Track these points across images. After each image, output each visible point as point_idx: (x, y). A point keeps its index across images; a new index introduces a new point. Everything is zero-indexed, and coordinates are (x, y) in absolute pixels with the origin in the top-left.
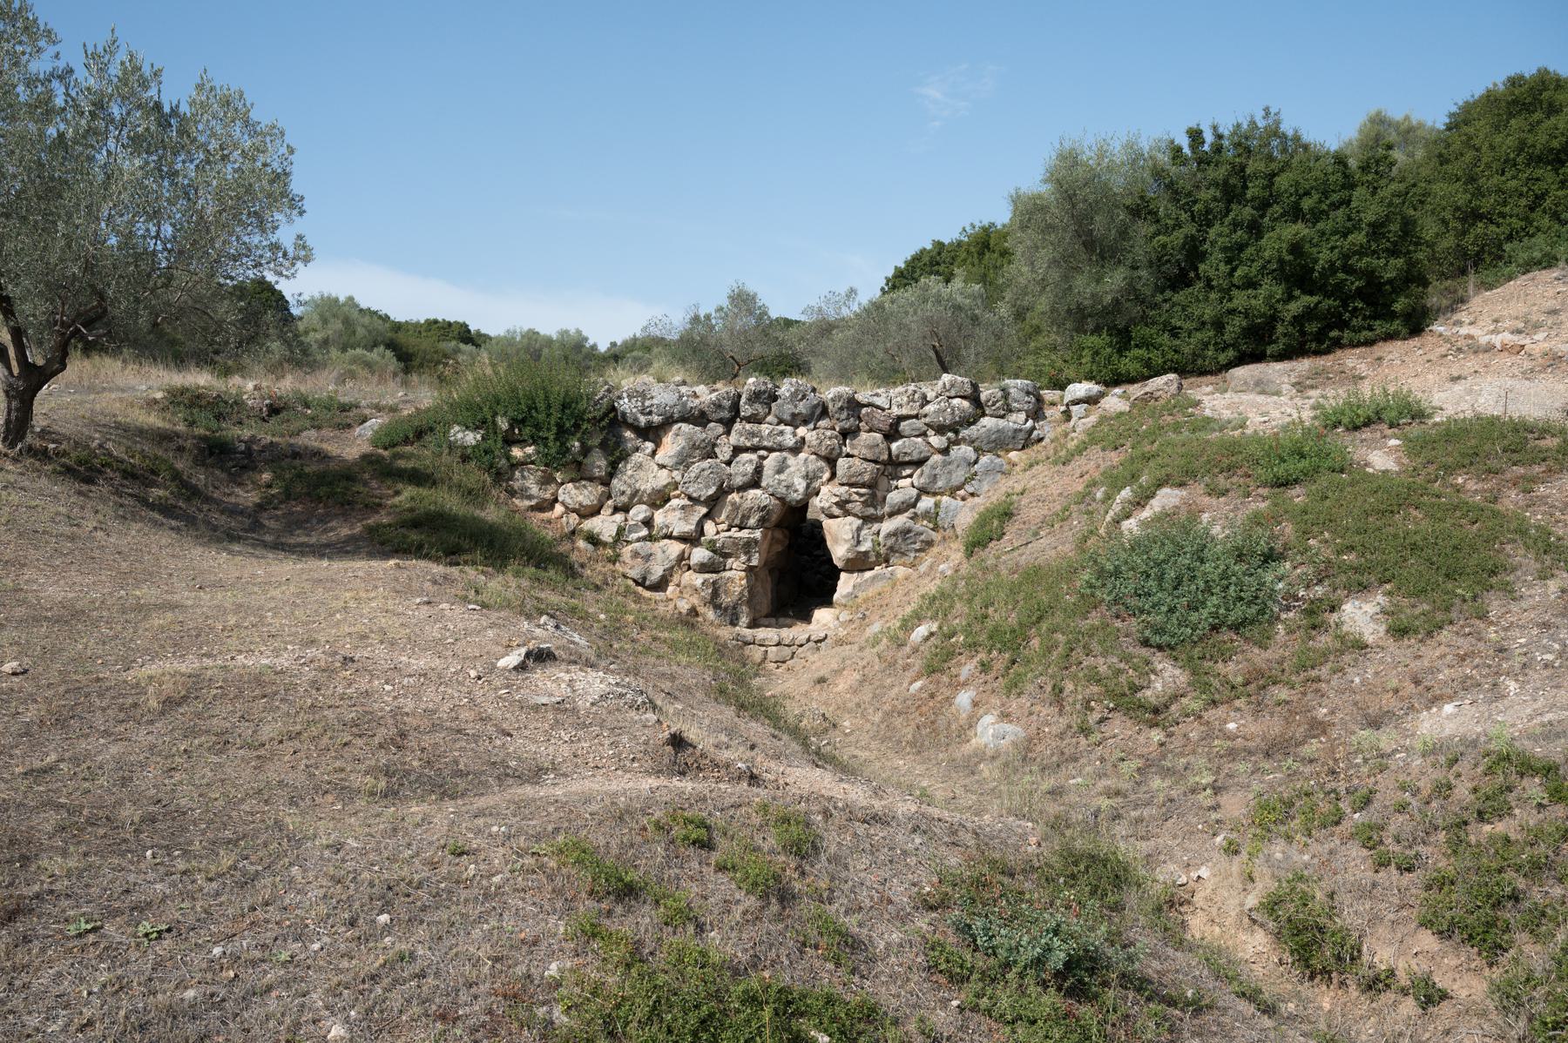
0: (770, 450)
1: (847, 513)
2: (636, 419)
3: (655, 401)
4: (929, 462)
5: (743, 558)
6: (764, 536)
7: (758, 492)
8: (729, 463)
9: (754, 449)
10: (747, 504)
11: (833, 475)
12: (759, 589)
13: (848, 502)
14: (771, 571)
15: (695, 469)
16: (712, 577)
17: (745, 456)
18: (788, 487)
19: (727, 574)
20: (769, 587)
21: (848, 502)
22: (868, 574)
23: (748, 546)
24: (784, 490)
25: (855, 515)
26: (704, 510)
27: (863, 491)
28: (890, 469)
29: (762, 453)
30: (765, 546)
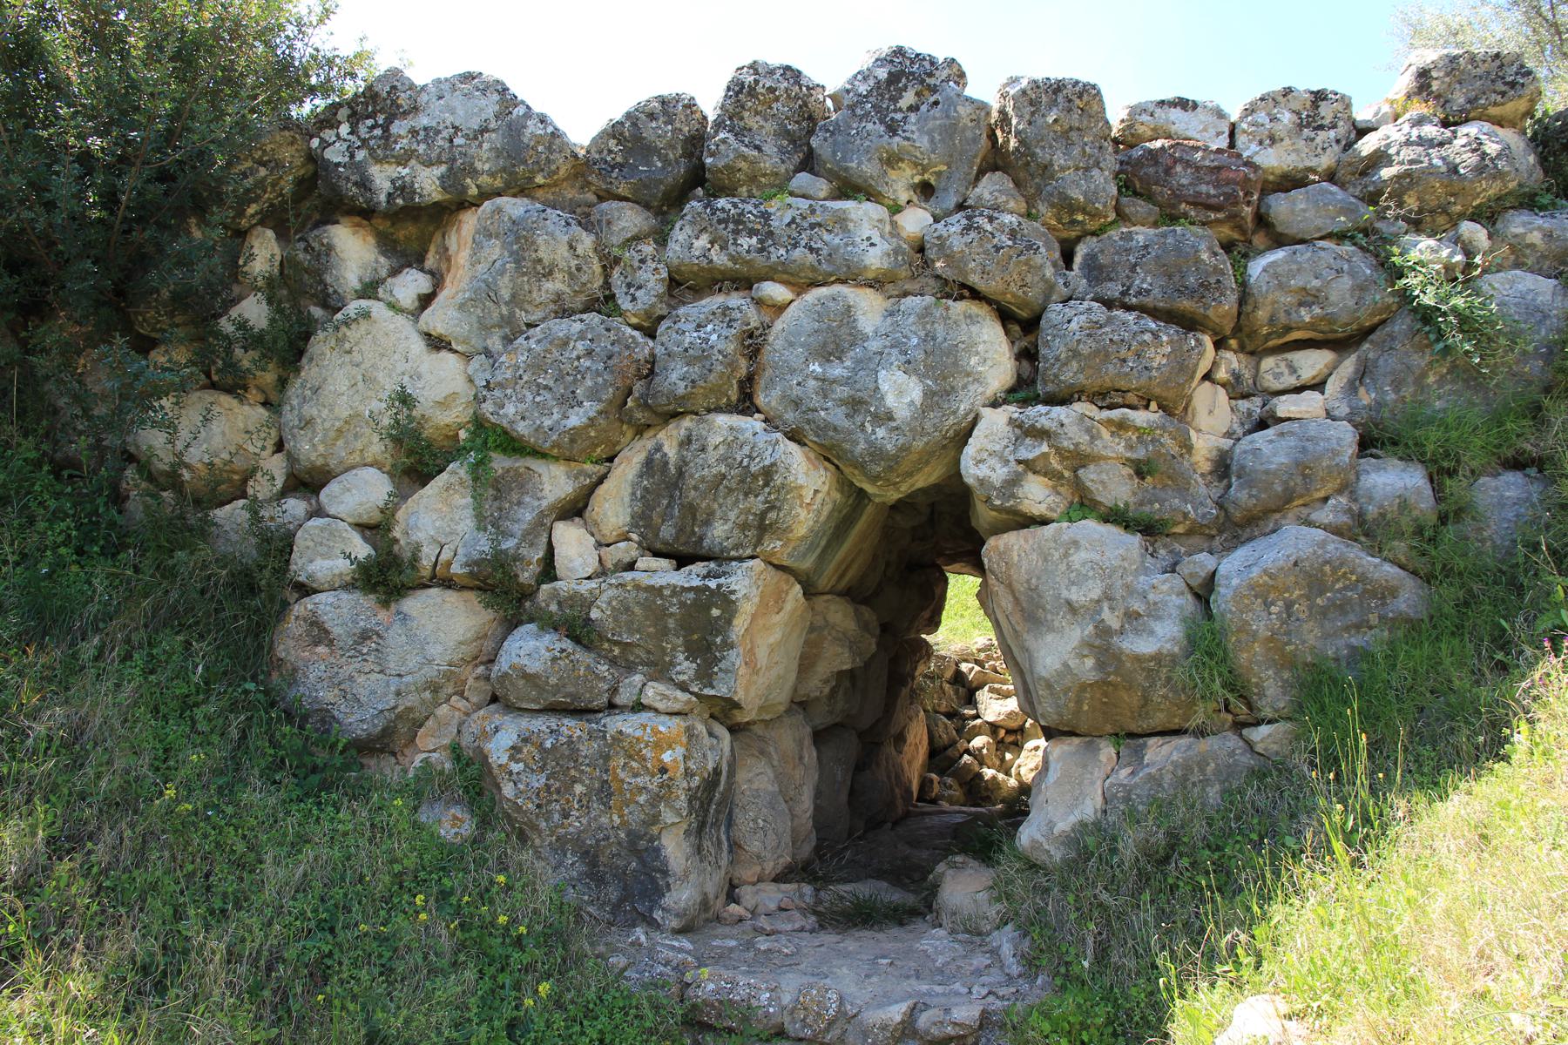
0: (802, 282)
1: (1084, 504)
2: (365, 184)
3: (423, 121)
5: (686, 668)
7: (752, 425)
9: (744, 282)
10: (709, 465)
15: (532, 343)
19: (626, 724)
22: (1159, 753)
25: (1114, 516)
26: (556, 482)
29: (774, 291)
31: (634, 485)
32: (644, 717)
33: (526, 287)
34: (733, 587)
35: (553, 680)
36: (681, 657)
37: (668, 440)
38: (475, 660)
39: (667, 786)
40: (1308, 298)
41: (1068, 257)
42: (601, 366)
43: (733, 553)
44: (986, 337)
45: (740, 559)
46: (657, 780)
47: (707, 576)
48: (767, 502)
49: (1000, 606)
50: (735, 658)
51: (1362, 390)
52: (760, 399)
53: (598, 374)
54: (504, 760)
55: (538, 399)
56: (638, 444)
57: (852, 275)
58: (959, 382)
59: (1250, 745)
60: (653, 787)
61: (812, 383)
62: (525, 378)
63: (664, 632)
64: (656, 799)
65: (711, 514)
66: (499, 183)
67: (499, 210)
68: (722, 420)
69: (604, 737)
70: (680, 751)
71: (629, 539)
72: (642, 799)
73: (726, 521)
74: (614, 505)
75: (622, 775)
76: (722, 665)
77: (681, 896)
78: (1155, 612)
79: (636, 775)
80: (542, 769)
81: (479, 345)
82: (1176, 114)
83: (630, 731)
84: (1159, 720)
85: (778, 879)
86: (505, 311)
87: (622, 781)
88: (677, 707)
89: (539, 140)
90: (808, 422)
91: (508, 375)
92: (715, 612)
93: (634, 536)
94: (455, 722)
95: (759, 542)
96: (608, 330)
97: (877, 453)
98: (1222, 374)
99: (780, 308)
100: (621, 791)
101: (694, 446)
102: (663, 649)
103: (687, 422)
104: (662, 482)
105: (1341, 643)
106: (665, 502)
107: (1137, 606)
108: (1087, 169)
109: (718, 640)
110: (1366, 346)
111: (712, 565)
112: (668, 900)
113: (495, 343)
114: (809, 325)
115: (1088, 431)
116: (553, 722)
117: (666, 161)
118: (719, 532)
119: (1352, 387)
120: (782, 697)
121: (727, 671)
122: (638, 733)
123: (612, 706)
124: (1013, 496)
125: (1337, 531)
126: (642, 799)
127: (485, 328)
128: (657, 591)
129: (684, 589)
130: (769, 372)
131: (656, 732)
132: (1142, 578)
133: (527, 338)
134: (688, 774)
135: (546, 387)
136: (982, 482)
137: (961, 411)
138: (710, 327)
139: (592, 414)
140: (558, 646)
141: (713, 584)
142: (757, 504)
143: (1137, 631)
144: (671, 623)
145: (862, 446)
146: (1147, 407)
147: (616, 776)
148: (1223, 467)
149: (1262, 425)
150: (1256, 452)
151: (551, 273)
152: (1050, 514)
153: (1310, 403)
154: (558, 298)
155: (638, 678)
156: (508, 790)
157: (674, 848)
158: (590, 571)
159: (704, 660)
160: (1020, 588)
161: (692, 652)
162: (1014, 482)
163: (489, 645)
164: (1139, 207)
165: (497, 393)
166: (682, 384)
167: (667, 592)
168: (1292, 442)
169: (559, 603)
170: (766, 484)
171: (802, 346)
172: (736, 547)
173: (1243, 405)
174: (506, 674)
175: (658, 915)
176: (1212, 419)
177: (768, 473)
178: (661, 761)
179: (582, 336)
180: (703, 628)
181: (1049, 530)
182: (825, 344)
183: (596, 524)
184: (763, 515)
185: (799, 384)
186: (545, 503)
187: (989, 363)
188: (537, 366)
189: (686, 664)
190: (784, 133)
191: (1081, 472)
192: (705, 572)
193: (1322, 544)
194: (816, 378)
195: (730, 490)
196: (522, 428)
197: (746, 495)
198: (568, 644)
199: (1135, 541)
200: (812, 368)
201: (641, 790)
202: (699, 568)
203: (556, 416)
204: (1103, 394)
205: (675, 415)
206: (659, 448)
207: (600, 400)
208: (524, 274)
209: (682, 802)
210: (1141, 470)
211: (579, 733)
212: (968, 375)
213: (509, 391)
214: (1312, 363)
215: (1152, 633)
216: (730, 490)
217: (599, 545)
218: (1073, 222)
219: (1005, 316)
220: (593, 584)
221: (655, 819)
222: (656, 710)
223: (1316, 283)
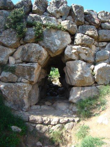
1: (79, 58)
5: (27, 77)
6: (38, 68)
11: (73, 40)
14: (39, 87)
18: (51, 43)
20: (38, 92)
26: (10, 51)
27: (87, 48)
37: (26, 46)
40: (105, 36)
41: (78, 28)
47: (31, 65)
49: (68, 70)
50: (34, 75)
54: (3, 89)
56: (21, 46)
59: (97, 88)
60: (23, 92)
66: (2, 8)
67: (3, 12)
68: (34, 44)
72: (22, 94)
73: (34, 57)
74: (18, 54)
76: (32, 76)
77: (27, 107)
82: (91, 12)
85: (36, 105)
89: (9, 3)
92: (32, 70)
95: (38, 60)
97: (54, 50)
98: (95, 44)
103: (29, 44)
104: (25, 52)
107: (86, 71)
108: (81, 17)
112: (25, 107)
116: (9, 84)
117: (27, 8)
118: (33, 59)
120: (36, 82)
123: (17, 82)
128: (24, 66)
134: (28, 91)
136: (67, 54)
141: (32, 66)
142: (38, 55)
144: (26, 71)
148: (95, 55)
150: (99, 54)
155: (20, 78)
156: (3, 93)
157: (26, 100)
158: (14, 63)
160: (71, 68)
161: (28, 75)
162: (72, 55)
164: (87, 23)
175: (23, 109)
177: (40, 51)
180: (30, 72)
181: (75, 61)
184: (39, 57)
190: (43, 7)
191: (80, 54)
195: (35, 53)
196: (5, 43)
202: (29, 64)
204: (83, 45)
205: (27, 43)
209: (27, 95)
214: (105, 44)
216: (35, 53)
217: (15, 60)
218: (79, 23)
219: (70, 34)
223: (106, 34)
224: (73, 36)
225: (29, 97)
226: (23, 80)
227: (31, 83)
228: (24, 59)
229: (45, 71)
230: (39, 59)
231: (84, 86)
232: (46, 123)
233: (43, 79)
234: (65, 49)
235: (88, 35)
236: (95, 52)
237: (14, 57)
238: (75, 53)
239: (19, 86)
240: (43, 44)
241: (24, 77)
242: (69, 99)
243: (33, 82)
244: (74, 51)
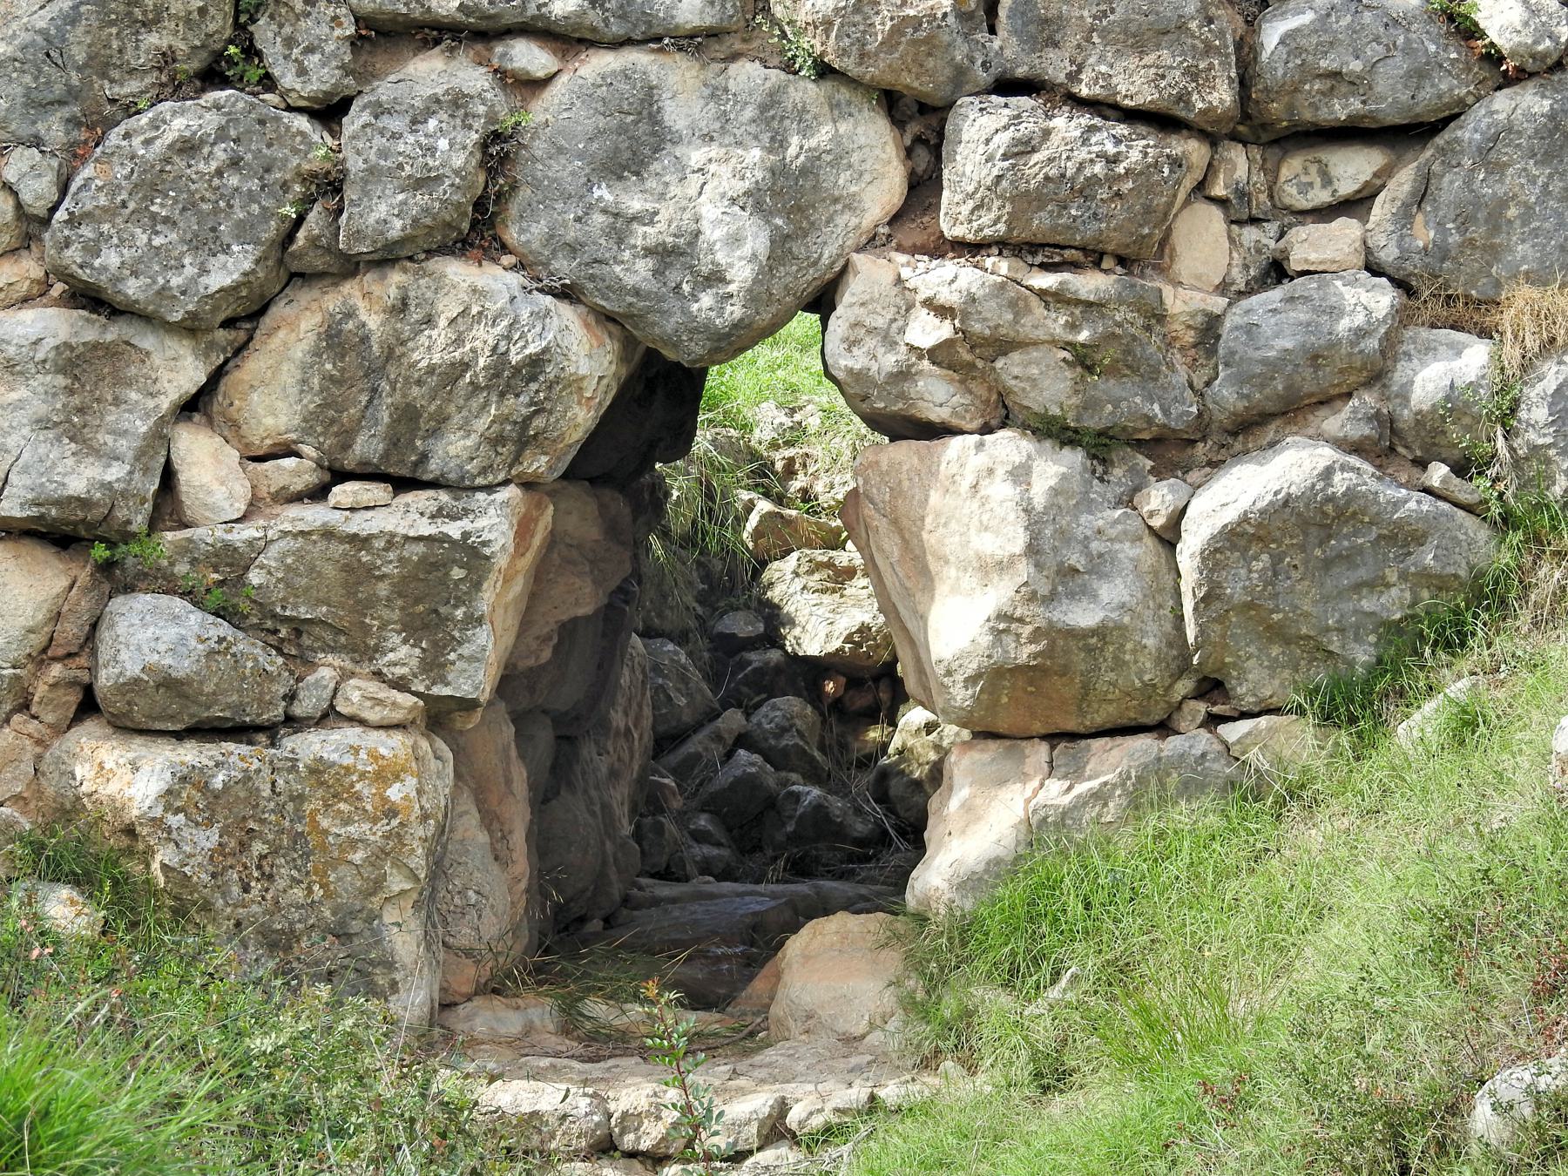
0: (569, 40)
1: (1002, 413)
4: (1468, 132)
5: (401, 655)
6: (523, 530)
8: (329, 112)
11: (923, 188)
12: (471, 829)
13: (1003, 346)
16: (227, 761)
17: (428, 73)
18: (664, 255)
19: (310, 745)
20: (518, 816)
21: (1003, 346)
22: (1111, 762)
23: (433, 588)
24: (640, 272)
26: (182, 371)
27: (1090, 284)
28: (1239, 164)
29: (529, 56)
30: (518, 586)
31: (305, 368)
32: (351, 734)
33: (115, 44)
34: (486, 536)
35: (209, 688)
36: (396, 639)
37: (365, 304)
38: (42, 657)
39: (397, 836)
42: (254, 184)
43: (480, 481)
44: (862, 140)
45: (489, 489)
46: (382, 827)
48: (532, 403)
51: (1420, 218)
52: (512, 234)
53: (251, 197)
54: (158, 812)
55: (157, 241)
56: (305, 295)
57: (656, 37)
58: (820, 215)
61: (598, 219)
62: (132, 205)
63: (370, 603)
64: (380, 855)
65: (442, 420)
69: (293, 769)
70: (411, 782)
71: (298, 455)
72: (358, 857)
75: (325, 823)
76: (466, 650)
78: (1100, 566)
79: (347, 822)
80: (210, 822)
81: (25, 131)
83: (334, 757)
84: (1101, 715)
86: (75, 78)
87: (326, 832)
88: (398, 716)
90: (592, 278)
91: (103, 201)
92: (457, 573)
93: (307, 449)
94: (28, 757)
95: (517, 460)
96: (262, 122)
99: (534, 85)
100: (324, 847)
101: (416, 315)
102: (366, 630)
105: (1348, 606)
106: (364, 398)
107: (1075, 559)
109: (459, 613)
110: (1428, 153)
111: (444, 497)
113: (54, 129)
114: (586, 120)
115: (1013, 304)
119: (1405, 217)
121: (472, 659)
122: (348, 760)
123: (293, 723)
124: (902, 396)
125: (1356, 448)
126: (358, 857)
127: (38, 105)
129: (407, 538)
130: (525, 193)
131: (375, 756)
132: (1084, 518)
133: (127, 136)
134: (425, 817)
135: (166, 220)
137: (825, 260)
138: (432, 124)
139: (247, 265)
140: (214, 633)
142: (518, 405)
143: (1071, 595)
145: (678, 318)
146: (1097, 265)
147: (314, 824)
149: (1277, 271)
150: (1250, 329)
151: (157, 20)
152: (955, 422)
153: (1336, 240)
154: (167, 58)
155: (326, 674)
159: (435, 644)
161: (413, 629)
162: (904, 375)
163: (71, 630)
165: (87, 231)
166: (398, 224)
167: (379, 544)
168: (1301, 314)
169: (194, 562)
170: (533, 378)
171: (581, 156)
172: (484, 471)
173: (1250, 234)
174: (137, 681)
176: (1205, 247)
177: (536, 363)
178: (385, 800)
179: (222, 134)
182: (617, 150)
183: (235, 425)
184: (528, 420)
185: (578, 220)
186: (165, 404)
187: (867, 177)
188: (151, 183)
189: (404, 651)
192: (432, 507)
193: (1327, 474)
194: (604, 211)
196: (133, 288)
197: (502, 395)
198: (224, 629)
199: (1074, 458)
200: (597, 193)
201: (353, 843)
202: (420, 499)
203: (190, 271)
206: (350, 314)
207: (257, 242)
208: (112, 23)
209: (418, 860)
210: (1084, 360)
211: (256, 765)
212: (836, 201)
213: (105, 227)
214: (1352, 168)
215: (1094, 597)
219: (892, 102)
220: (248, 532)
221: (378, 884)
222: (363, 722)
223: (1356, 66)
224: (922, 123)
225: (433, 899)
226: (354, 696)
227: (439, 717)
228: (346, 447)
229: (602, 507)
230: (523, 438)
231: (1071, 725)
232: (645, 1145)
233: (568, 630)
234: (822, 302)
235: (1104, 108)
236: (1218, 303)
237: (232, 430)
238: (939, 354)
239: (318, 769)
240: (565, 268)
241: (363, 650)
242: (908, 896)
243: (468, 705)
244: (927, 331)
